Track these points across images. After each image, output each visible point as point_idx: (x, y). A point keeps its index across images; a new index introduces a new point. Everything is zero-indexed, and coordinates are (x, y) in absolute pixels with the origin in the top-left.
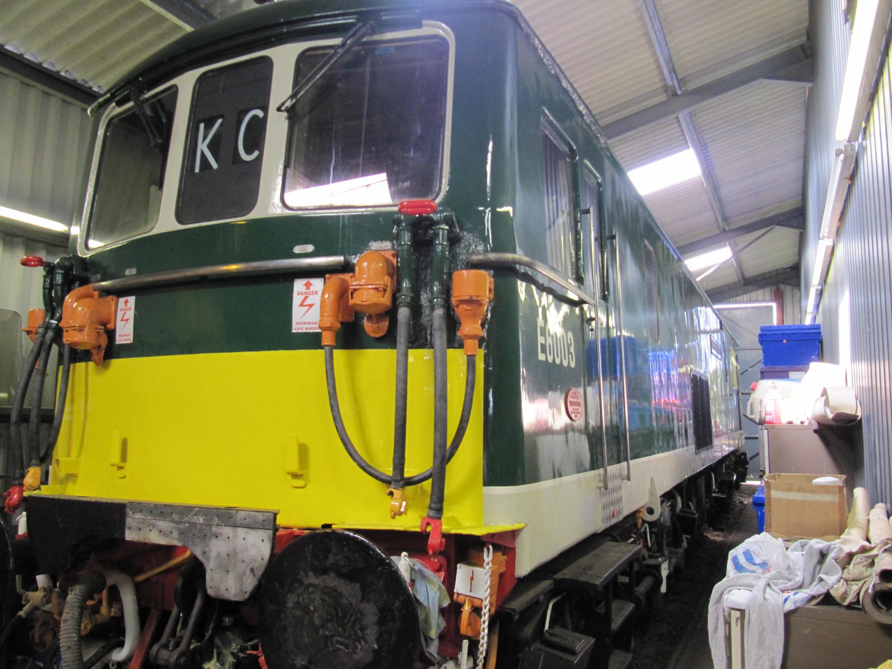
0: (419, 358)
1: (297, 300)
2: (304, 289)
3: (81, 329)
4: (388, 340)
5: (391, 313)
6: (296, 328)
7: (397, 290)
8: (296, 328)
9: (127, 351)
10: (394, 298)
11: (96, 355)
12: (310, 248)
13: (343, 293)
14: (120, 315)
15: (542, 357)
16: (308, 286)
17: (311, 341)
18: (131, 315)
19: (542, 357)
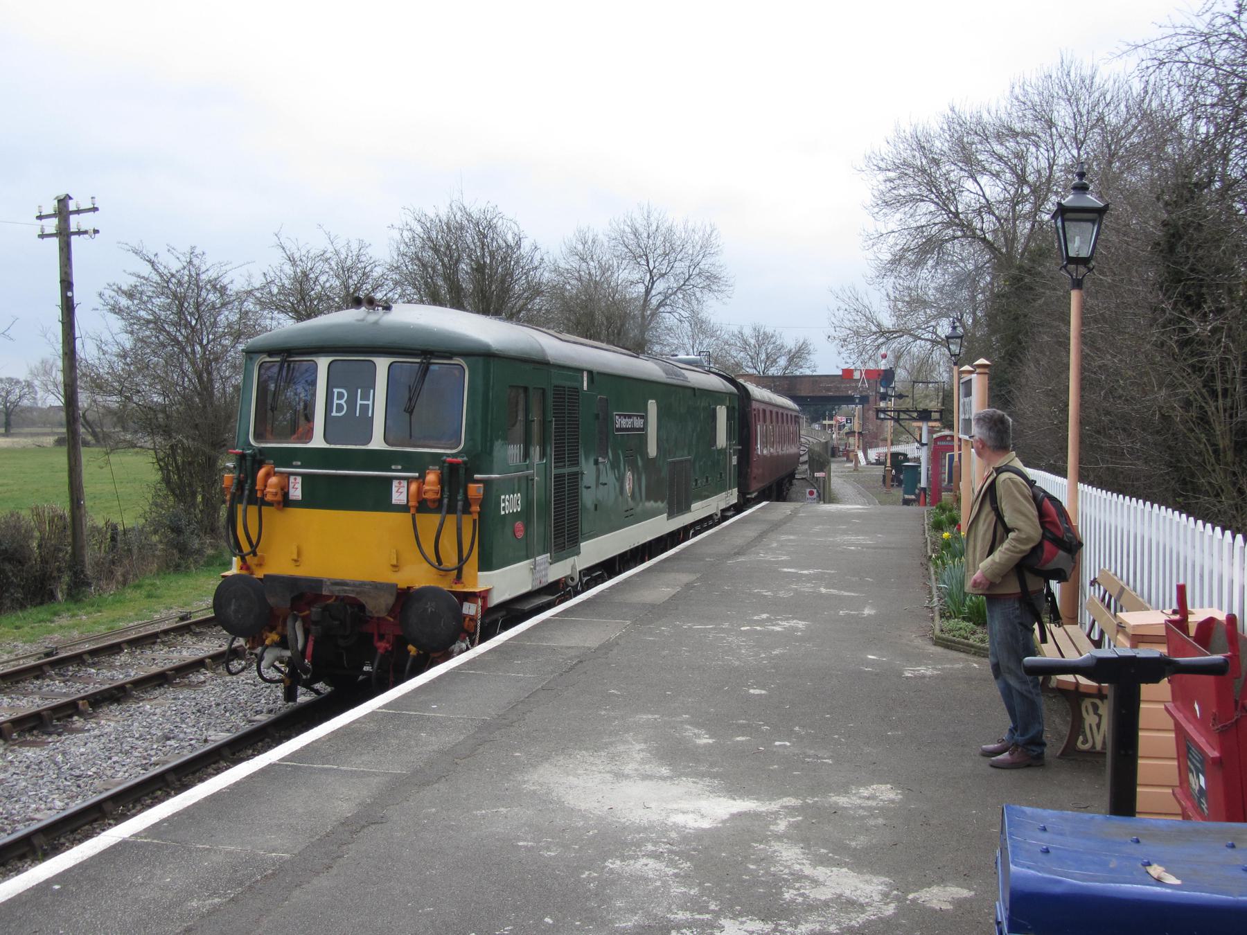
0: (451, 520)
1: (394, 489)
2: (398, 485)
3: (276, 494)
4: (438, 510)
5: (440, 501)
6: (394, 502)
7: (442, 490)
8: (394, 502)
9: (296, 504)
10: (442, 495)
11: (275, 505)
13: (419, 490)
14: (291, 485)
15: (503, 513)
16: (400, 483)
17: (404, 508)
18: (299, 486)
19: (503, 513)
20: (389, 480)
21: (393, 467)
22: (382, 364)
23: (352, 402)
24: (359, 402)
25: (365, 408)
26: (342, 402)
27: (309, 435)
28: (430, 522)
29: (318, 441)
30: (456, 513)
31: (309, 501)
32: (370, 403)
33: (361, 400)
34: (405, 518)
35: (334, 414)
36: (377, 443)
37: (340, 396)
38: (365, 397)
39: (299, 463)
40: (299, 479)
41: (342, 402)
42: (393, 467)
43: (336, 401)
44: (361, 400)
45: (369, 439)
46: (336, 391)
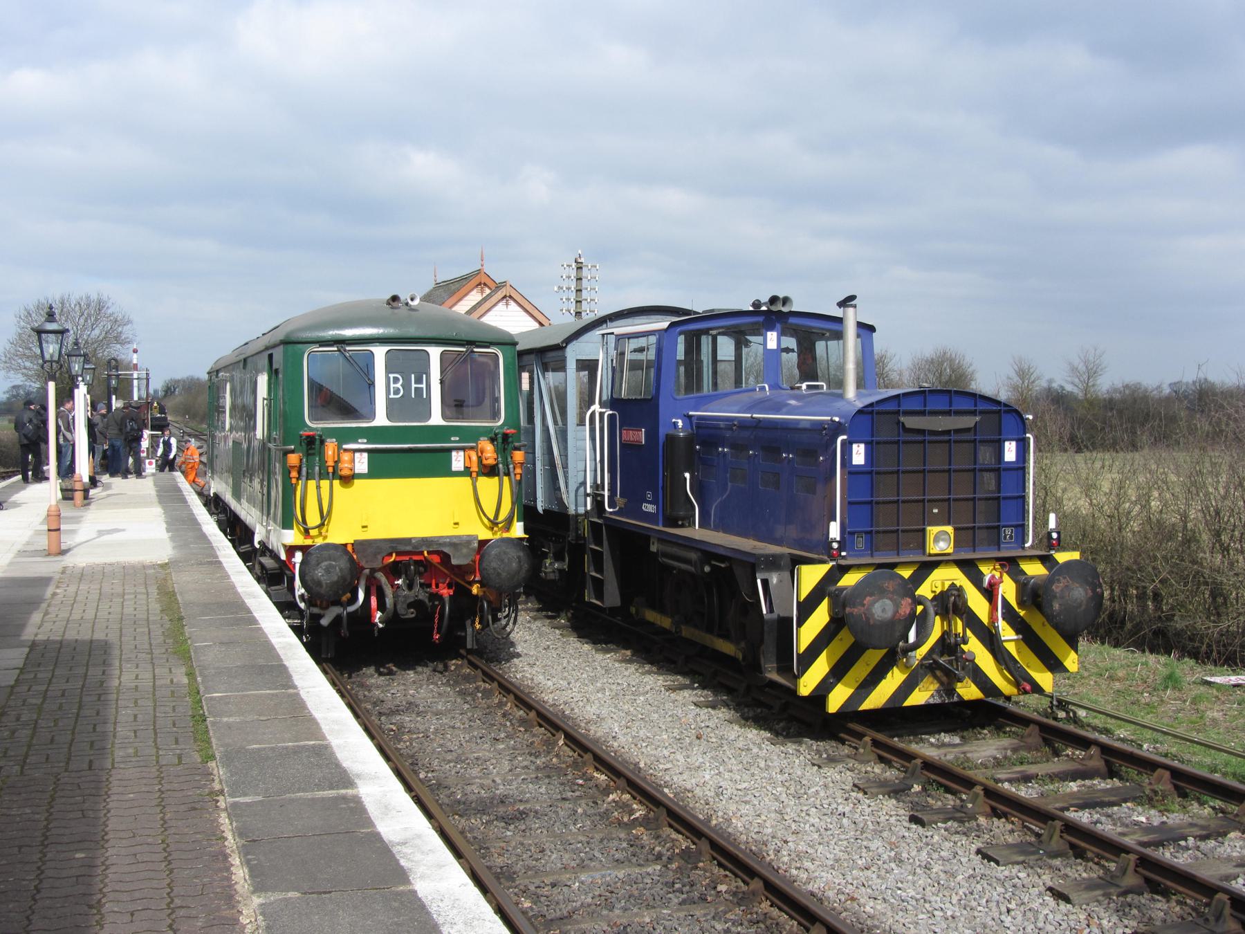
9: (361, 476)
12: (458, 439)
20: (449, 450)
21: (452, 439)
22: (435, 352)
23: (406, 386)
24: (414, 386)
25: (418, 390)
26: (399, 385)
27: (372, 416)
28: (488, 486)
29: (381, 419)
30: (498, 475)
31: (374, 473)
32: (424, 386)
33: (415, 383)
34: (466, 481)
35: (392, 396)
36: (436, 419)
37: (396, 380)
38: (419, 381)
39: (365, 441)
40: (365, 455)
41: (399, 385)
42: (452, 439)
43: (392, 386)
44: (415, 383)
45: (429, 416)
46: (391, 376)
